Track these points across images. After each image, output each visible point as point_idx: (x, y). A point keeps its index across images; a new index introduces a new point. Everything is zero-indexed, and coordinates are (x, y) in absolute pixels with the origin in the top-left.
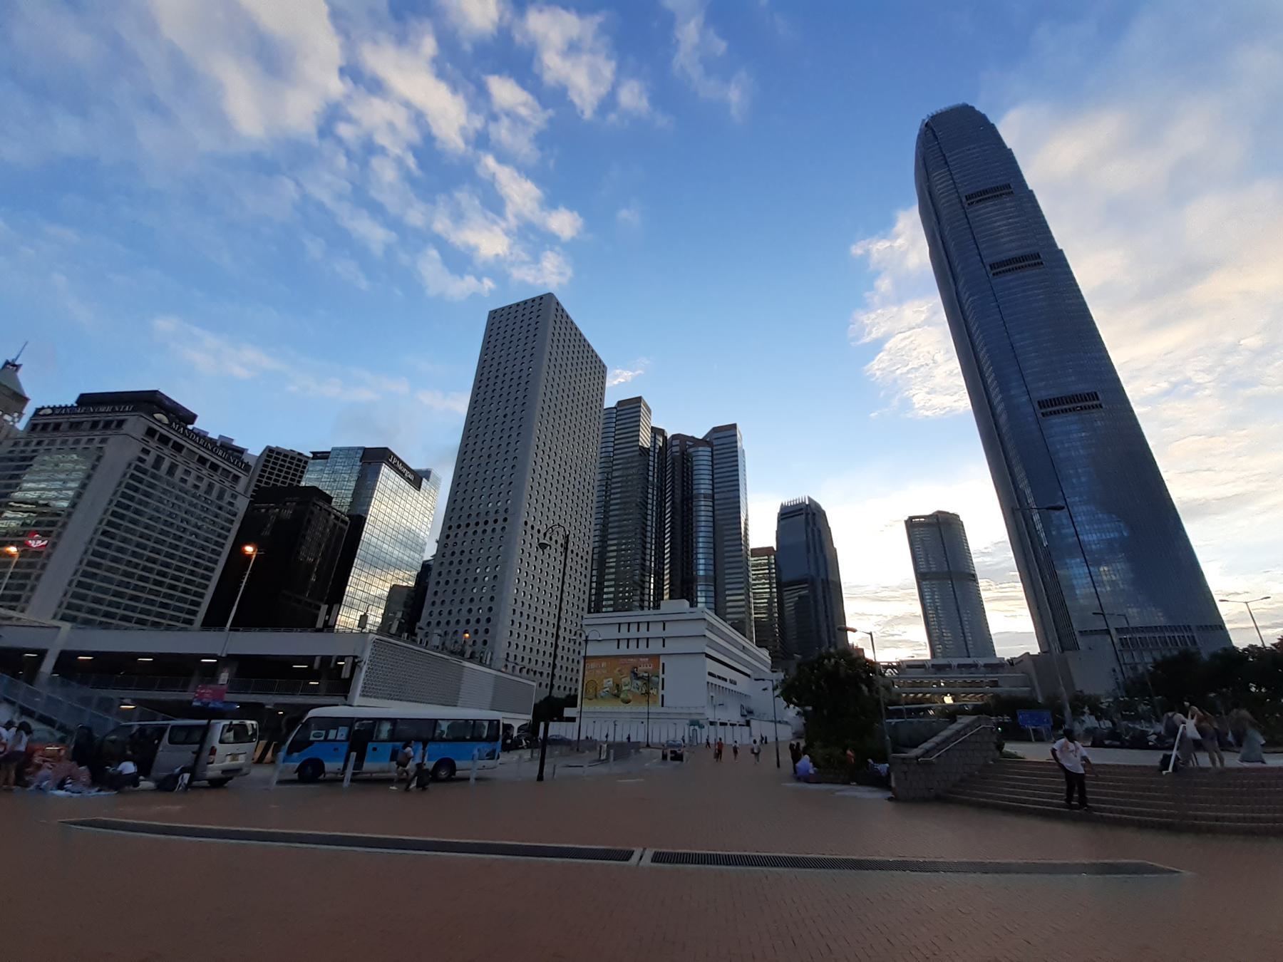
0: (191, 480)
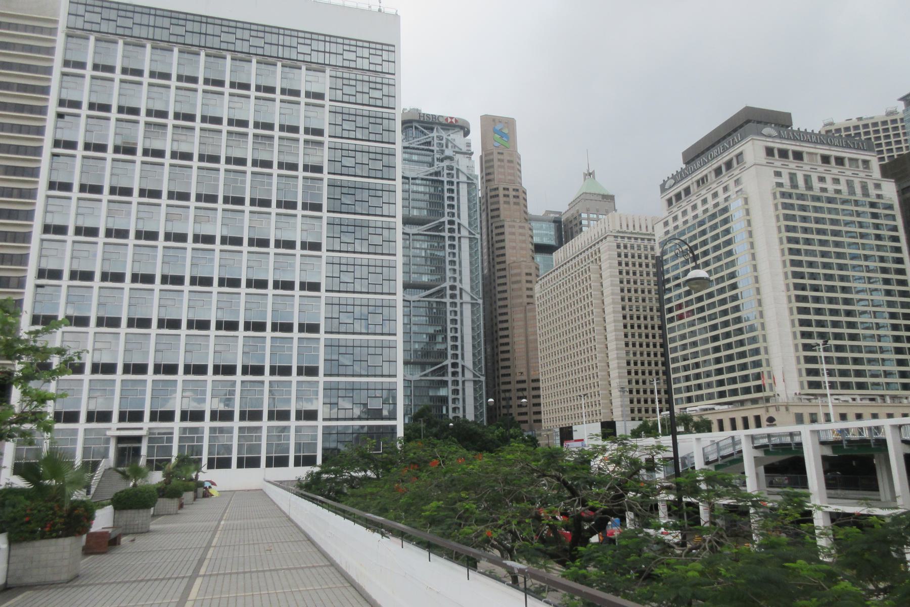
0: (830, 186)
